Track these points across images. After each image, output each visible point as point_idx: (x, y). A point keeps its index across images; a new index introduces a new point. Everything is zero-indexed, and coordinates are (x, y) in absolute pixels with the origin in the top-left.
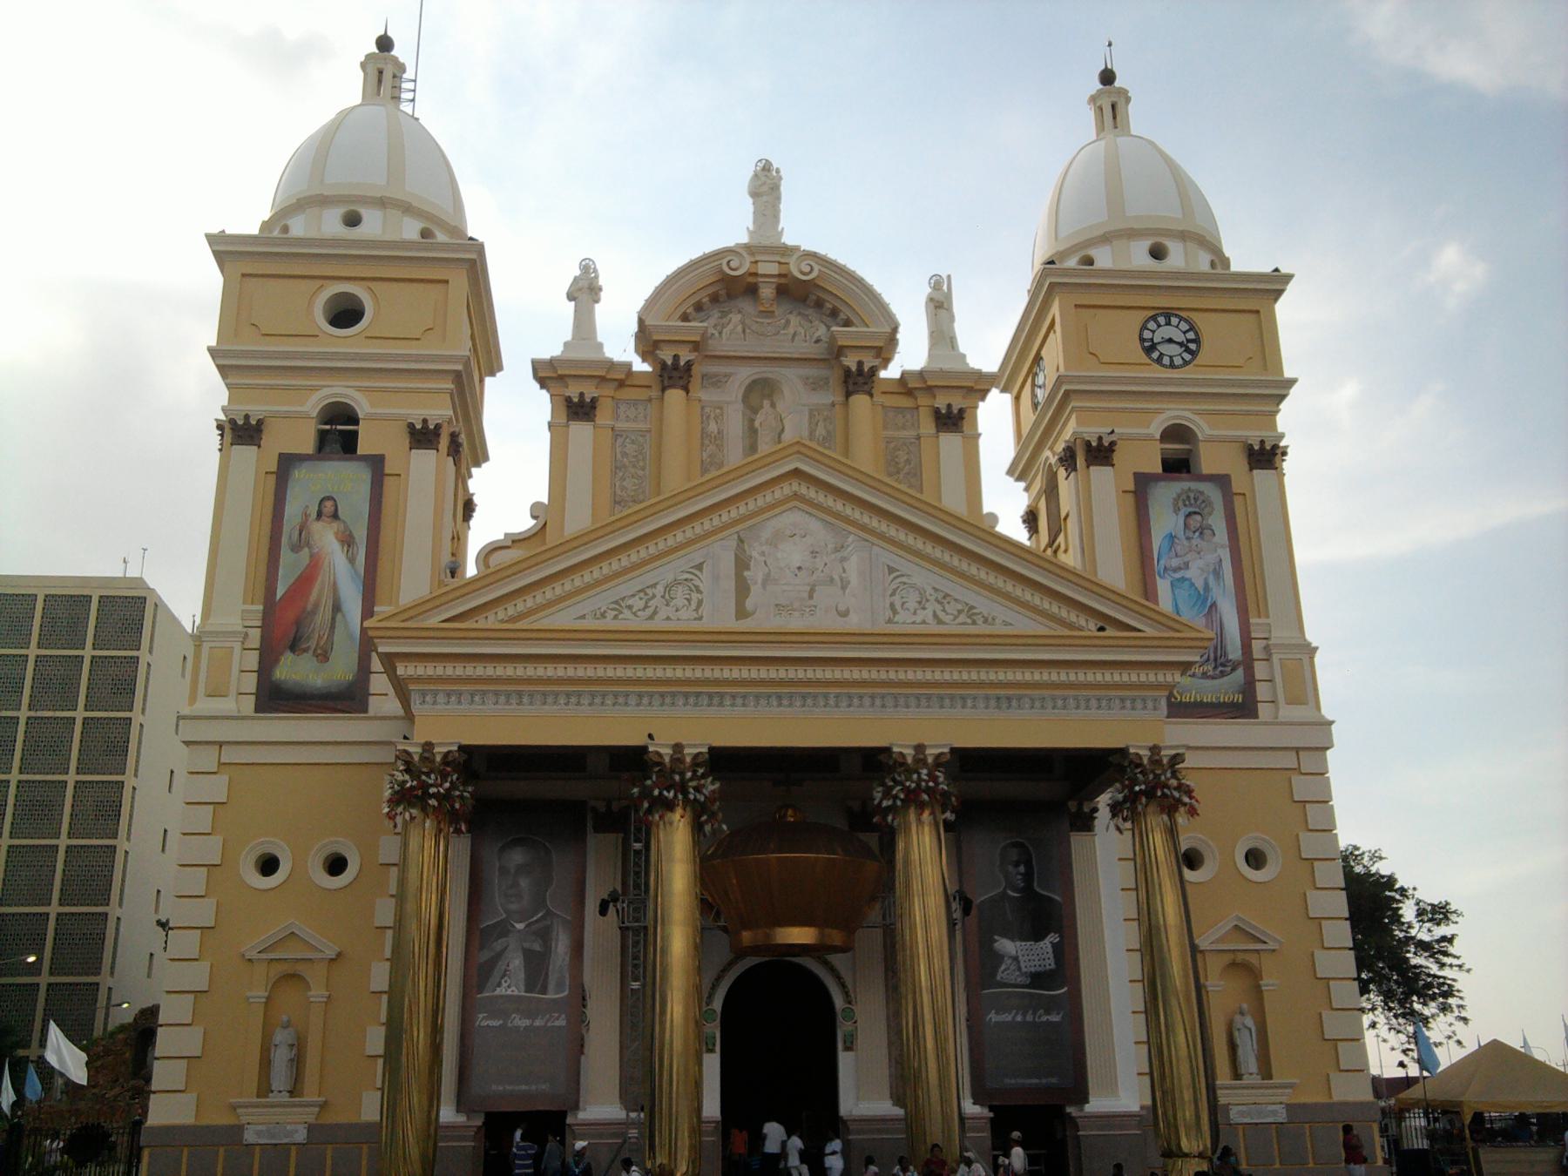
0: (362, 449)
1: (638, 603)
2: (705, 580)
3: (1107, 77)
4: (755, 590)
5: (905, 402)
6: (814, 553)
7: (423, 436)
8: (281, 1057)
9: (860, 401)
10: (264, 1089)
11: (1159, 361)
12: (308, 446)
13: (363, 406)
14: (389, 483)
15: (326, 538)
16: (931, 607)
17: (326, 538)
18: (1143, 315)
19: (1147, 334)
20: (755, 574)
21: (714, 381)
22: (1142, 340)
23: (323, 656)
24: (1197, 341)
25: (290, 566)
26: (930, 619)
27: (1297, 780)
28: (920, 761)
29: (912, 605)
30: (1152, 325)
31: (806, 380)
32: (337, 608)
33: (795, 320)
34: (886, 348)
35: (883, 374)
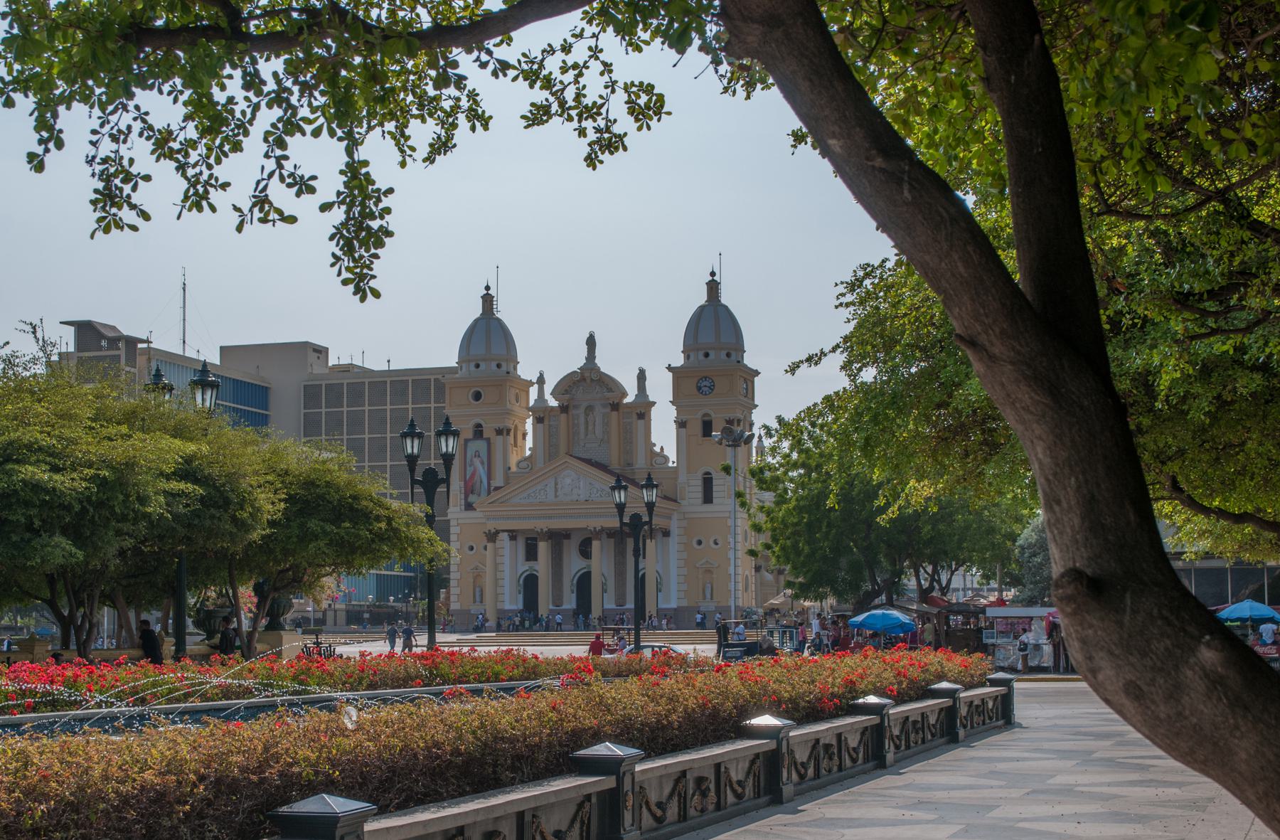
0: (485, 435)
7: (499, 432)
9: (615, 413)
10: (475, 602)
12: (470, 435)
13: (482, 423)
15: (477, 462)
17: (477, 462)
20: (559, 486)
21: (576, 407)
23: (479, 495)
25: (469, 470)
34: (625, 394)
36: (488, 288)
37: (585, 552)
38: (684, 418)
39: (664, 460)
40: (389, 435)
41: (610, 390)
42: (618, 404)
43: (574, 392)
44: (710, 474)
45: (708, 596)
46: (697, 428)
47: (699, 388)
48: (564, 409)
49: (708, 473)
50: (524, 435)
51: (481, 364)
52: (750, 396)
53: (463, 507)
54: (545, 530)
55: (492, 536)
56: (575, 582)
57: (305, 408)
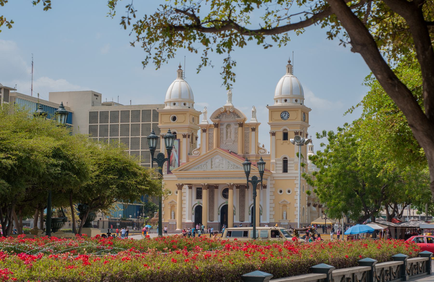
1: (200, 167)
2: (208, 164)
3: (289, 62)
4: (213, 165)
5: (248, 127)
6: (220, 160)
7: (184, 136)
8: (173, 215)
9: (240, 128)
10: (171, 218)
11: (283, 119)
13: (177, 133)
14: (181, 143)
16: (233, 166)
18: (281, 112)
19: (282, 115)
20: (213, 163)
21: (222, 125)
22: (281, 116)
23: (174, 167)
24: (289, 115)
26: (232, 167)
27: (295, 181)
28: (230, 185)
29: (230, 166)
30: (283, 113)
31: (234, 124)
32: (175, 160)
33: (233, 115)
34: (245, 119)
35: (246, 122)
36: (180, 67)
37: (225, 194)
38: (274, 131)
39: (264, 151)
40: (130, 137)
41: (239, 117)
42: (242, 124)
43: (221, 117)
44: (286, 158)
45: (285, 217)
46: (280, 136)
47: (282, 118)
48: (216, 126)
49: (286, 158)
50: (197, 138)
51: (177, 104)
52: (306, 120)
53: (166, 172)
54: (206, 184)
55: (180, 187)
56: (220, 209)
57: (90, 123)
